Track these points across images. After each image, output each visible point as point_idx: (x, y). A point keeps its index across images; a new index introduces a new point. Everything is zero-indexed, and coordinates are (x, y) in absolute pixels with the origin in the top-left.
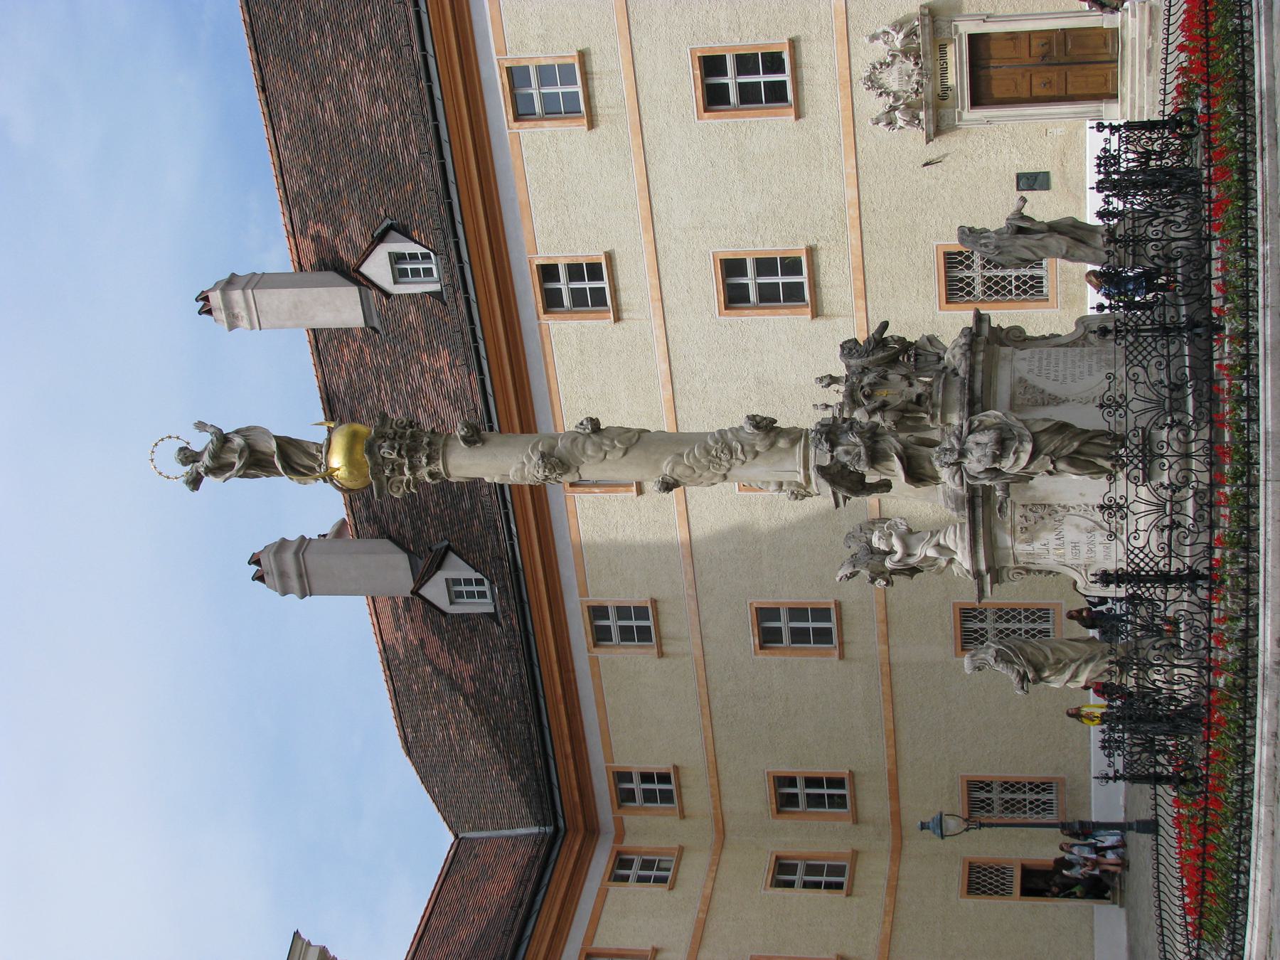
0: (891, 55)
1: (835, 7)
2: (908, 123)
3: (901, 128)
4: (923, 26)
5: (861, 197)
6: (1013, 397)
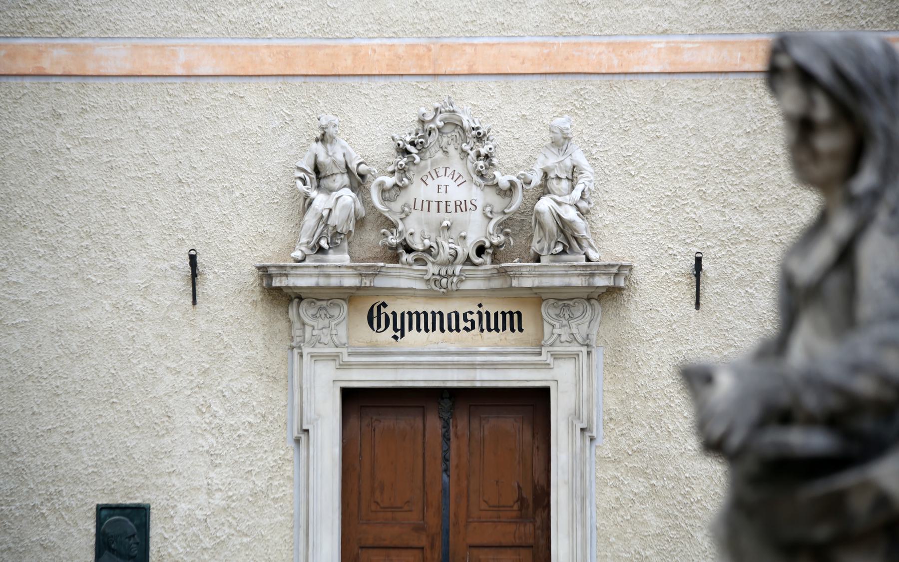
0: (512, 184)
1: (646, 44)
2: (323, 220)
3: (308, 202)
4: (591, 268)
5: (99, 82)
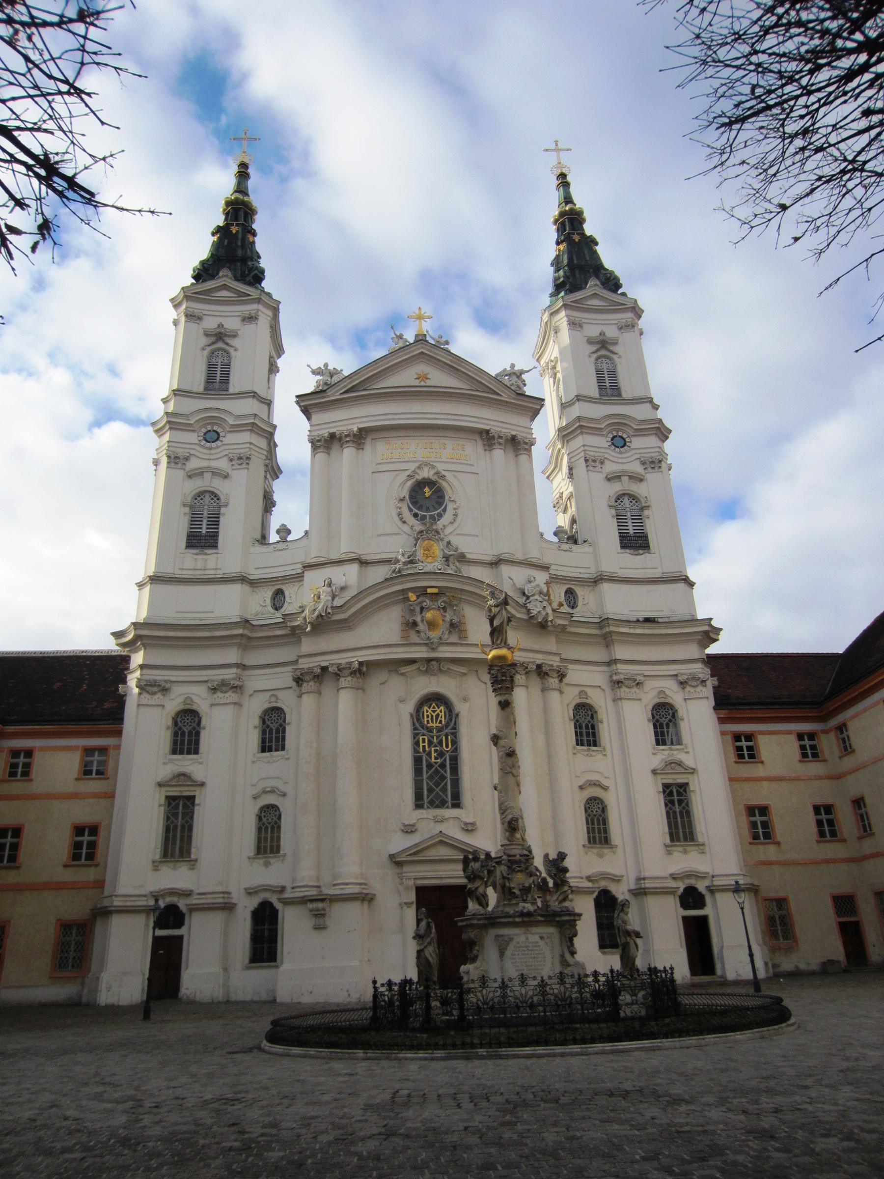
6: (502, 936)
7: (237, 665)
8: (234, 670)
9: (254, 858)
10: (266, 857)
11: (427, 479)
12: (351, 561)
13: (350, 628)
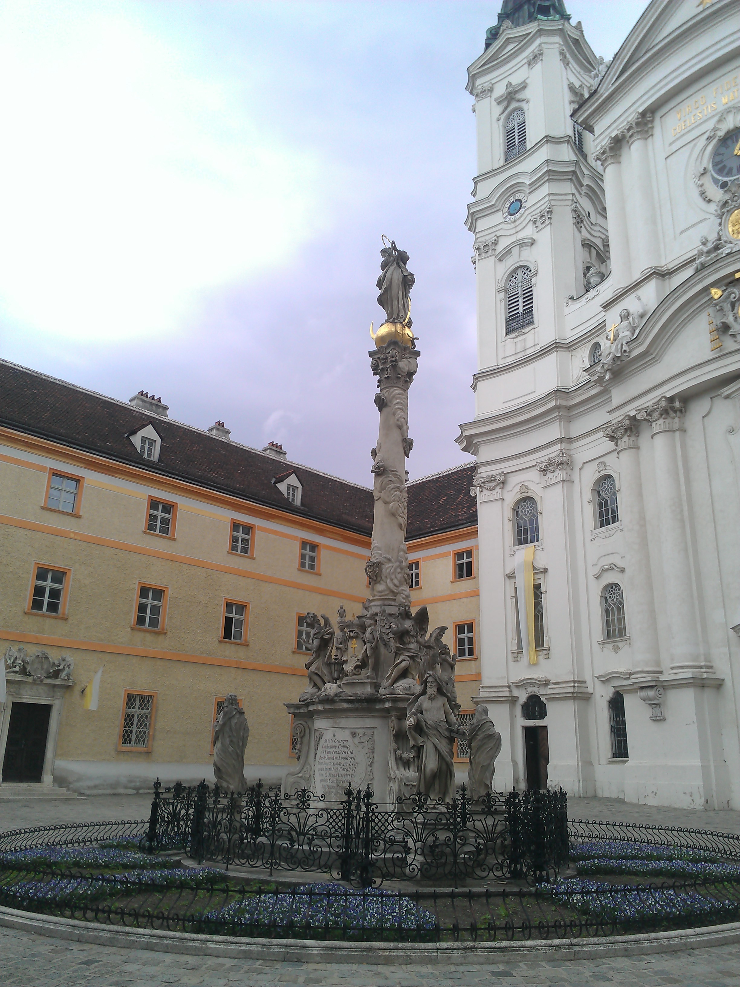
7: (561, 440)
8: (558, 447)
9: (604, 643)
10: (613, 642)
11: (733, 130)
12: (646, 279)
13: (655, 361)
